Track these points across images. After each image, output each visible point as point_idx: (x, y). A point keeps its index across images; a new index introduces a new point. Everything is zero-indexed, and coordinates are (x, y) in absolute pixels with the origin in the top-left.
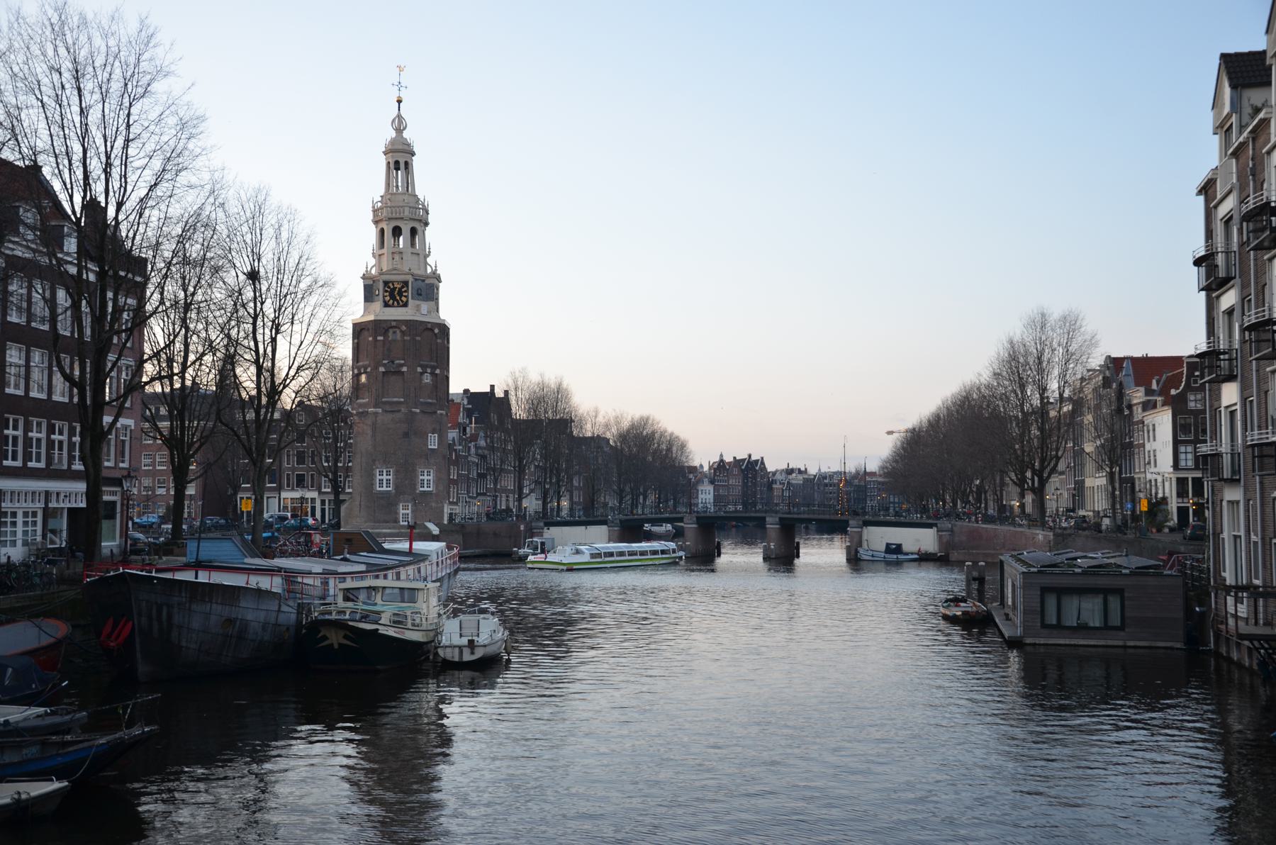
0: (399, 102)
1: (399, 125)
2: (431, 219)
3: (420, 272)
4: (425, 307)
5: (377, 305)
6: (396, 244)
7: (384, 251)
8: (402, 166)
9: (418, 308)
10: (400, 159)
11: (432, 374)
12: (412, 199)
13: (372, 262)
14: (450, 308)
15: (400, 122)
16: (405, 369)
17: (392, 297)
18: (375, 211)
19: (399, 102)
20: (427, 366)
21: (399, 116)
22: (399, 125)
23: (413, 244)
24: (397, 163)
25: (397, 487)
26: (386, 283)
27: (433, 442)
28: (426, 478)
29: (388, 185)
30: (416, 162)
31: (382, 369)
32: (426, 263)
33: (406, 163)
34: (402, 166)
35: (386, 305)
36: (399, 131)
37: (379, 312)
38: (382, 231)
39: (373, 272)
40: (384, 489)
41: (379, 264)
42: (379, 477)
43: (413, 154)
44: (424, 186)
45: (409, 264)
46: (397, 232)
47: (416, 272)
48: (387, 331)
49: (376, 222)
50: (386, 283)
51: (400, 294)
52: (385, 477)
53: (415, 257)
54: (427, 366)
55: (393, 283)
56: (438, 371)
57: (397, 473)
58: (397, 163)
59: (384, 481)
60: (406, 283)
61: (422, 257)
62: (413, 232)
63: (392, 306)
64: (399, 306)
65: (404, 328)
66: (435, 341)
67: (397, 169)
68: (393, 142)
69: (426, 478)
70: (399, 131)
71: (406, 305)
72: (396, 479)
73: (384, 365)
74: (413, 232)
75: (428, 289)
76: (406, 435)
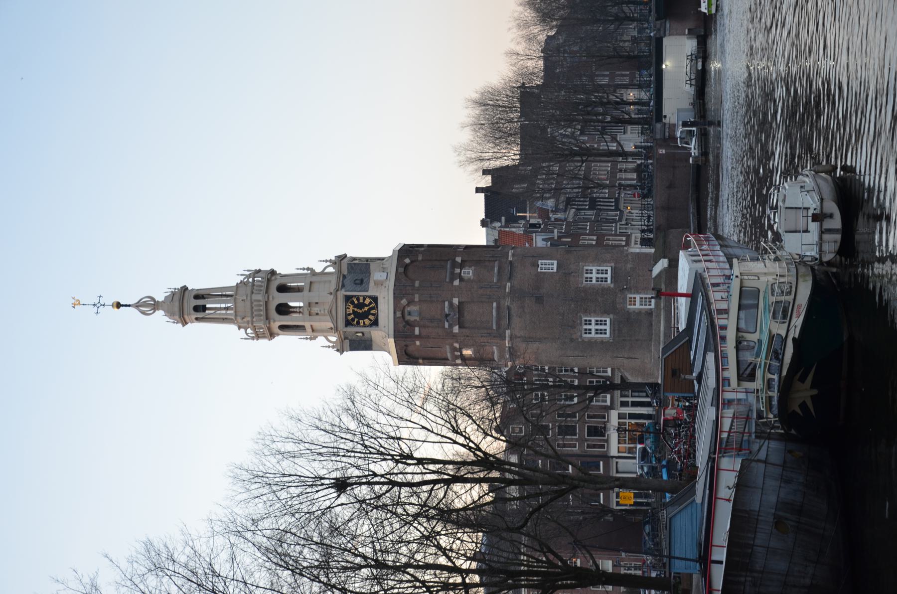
1: (148, 305)
2: (266, 267)
3: (334, 280)
4: (377, 275)
5: (376, 334)
6: (299, 310)
7: (307, 325)
8: (200, 302)
9: (379, 284)
10: (190, 305)
11: (462, 266)
12: (242, 290)
13: (321, 340)
14: (379, 243)
15: (145, 304)
16: (456, 301)
17: (365, 315)
18: (258, 336)
19: (119, 305)
20: (452, 273)
21: (137, 306)
22: (148, 305)
23: (299, 290)
24: (197, 309)
25: (606, 312)
26: (348, 323)
27: (549, 266)
28: (594, 275)
29: (224, 320)
31: (456, 329)
32: (323, 273)
33: (197, 297)
34: (200, 302)
35: (375, 323)
36: (155, 305)
37: (384, 331)
38: (283, 328)
39: (334, 339)
40: (608, 327)
41: (324, 332)
42: (593, 335)
43: (185, 289)
44: (223, 274)
45: (324, 295)
46: (283, 309)
47: (333, 287)
48: (408, 323)
49: (272, 335)
50: (348, 323)
51: (361, 306)
52: (593, 327)
53: (315, 286)
54: (452, 273)
55: (347, 315)
56: (459, 259)
57: (587, 312)
59: (597, 327)
60: (348, 299)
61: (314, 279)
62: (283, 289)
63: (376, 316)
64: (376, 308)
65: (404, 302)
66: (420, 264)
67: (204, 308)
68: (170, 314)
69: (594, 275)
70: (155, 305)
71: (375, 299)
72: (595, 313)
73: (451, 326)
74: (283, 289)
75: (354, 271)
76: (539, 300)
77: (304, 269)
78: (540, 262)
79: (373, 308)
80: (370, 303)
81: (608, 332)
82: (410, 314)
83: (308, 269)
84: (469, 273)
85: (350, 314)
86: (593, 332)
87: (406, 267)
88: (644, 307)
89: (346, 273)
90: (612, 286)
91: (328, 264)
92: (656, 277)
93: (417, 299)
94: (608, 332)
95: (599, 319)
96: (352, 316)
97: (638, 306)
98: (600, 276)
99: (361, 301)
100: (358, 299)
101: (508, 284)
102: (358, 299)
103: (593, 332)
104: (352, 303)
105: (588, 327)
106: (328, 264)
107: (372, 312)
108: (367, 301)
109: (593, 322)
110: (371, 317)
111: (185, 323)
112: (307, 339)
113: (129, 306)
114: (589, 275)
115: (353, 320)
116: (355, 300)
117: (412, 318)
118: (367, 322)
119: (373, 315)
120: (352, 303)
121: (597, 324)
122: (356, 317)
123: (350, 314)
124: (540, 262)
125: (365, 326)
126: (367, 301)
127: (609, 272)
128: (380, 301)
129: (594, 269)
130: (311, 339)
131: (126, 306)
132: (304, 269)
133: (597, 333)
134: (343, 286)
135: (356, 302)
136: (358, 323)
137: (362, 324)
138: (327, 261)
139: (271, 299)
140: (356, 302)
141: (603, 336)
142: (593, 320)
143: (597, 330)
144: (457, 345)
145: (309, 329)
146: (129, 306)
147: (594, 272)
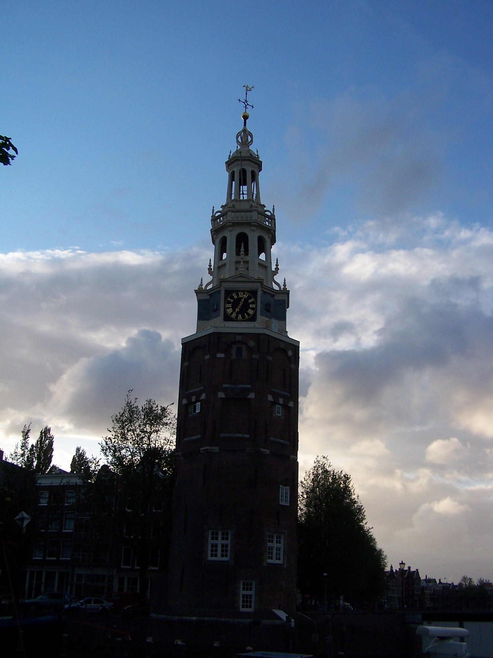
0: (246, 118)
13: (208, 278)
16: (252, 396)
18: (214, 219)
19: (246, 118)
21: (245, 130)
24: (243, 172)
26: (228, 293)
29: (230, 194)
30: (262, 176)
31: (221, 395)
35: (227, 318)
40: (219, 558)
42: (210, 541)
51: (246, 306)
52: (220, 542)
55: (237, 292)
56: (291, 404)
58: (243, 172)
60: (253, 293)
63: (236, 320)
64: (244, 320)
65: (252, 343)
67: (243, 182)
69: (275, 545)
73: (225, 390)
77: (277, 265)
78: (289, 488)
79: (243, 317)
80: (248, 314)
81: (214, 558)
82: (239, 350)
83: (277, 269)
84: (278, 413)
85: (238, 295)
86: (215, 542)
87: (285, 351)
88: (241, 599)
89: (276, 298)
90: (265, 564)
91: (282, 287)
92: (274, 614)
93: (254, 356)
94: (214, 558)
95: (229, 548)
96: (236, 297)
97: (242, 592)
98: (275, 552)
99: (251, 306)
100: (253, 303)
101: (268, 452)
102: (253, 303)
103: (215, 542)
104: (249, 298)
105: (220, 536)
106: (282, 287)
107: (240, 317)
108: (251, 312)
109: (225, 542)
110: (234, 315)
111: (229, 164)
112: (210, 266)
113: (245, 125)
114: (275, 539)
115: (232, 297)
116: (252, 300)
117: (234, 352)
118: (230, 311)
119: (237, 317)
120: (249, 298)
121: (223, 546)
122: (235, 300)
123: (238, 295)
124: (289, 488)
125: (225, 309)
126: (251, 312)
127: (278, 562)
128: (251, 324)
129: (281, 545)
130: (210, 269)
131: (245, 123)
132: (277, 265)
133: (212, 546)
134: (265, 293)
135: (250, 301)
136: (229, 302)
137: (227, 306)
138: (285, 285)
139: (252, 228)
140: (250, 301)
141: (209, 553)
142: (228, 542)
143: (216, 546)
144: (203, 396)
145: (221, 263)
146: (245, 125)
147: (279, 545)
